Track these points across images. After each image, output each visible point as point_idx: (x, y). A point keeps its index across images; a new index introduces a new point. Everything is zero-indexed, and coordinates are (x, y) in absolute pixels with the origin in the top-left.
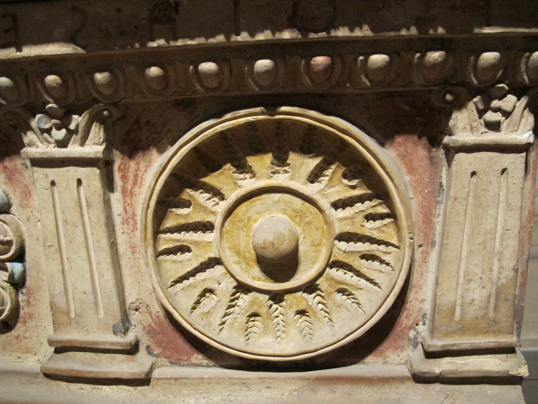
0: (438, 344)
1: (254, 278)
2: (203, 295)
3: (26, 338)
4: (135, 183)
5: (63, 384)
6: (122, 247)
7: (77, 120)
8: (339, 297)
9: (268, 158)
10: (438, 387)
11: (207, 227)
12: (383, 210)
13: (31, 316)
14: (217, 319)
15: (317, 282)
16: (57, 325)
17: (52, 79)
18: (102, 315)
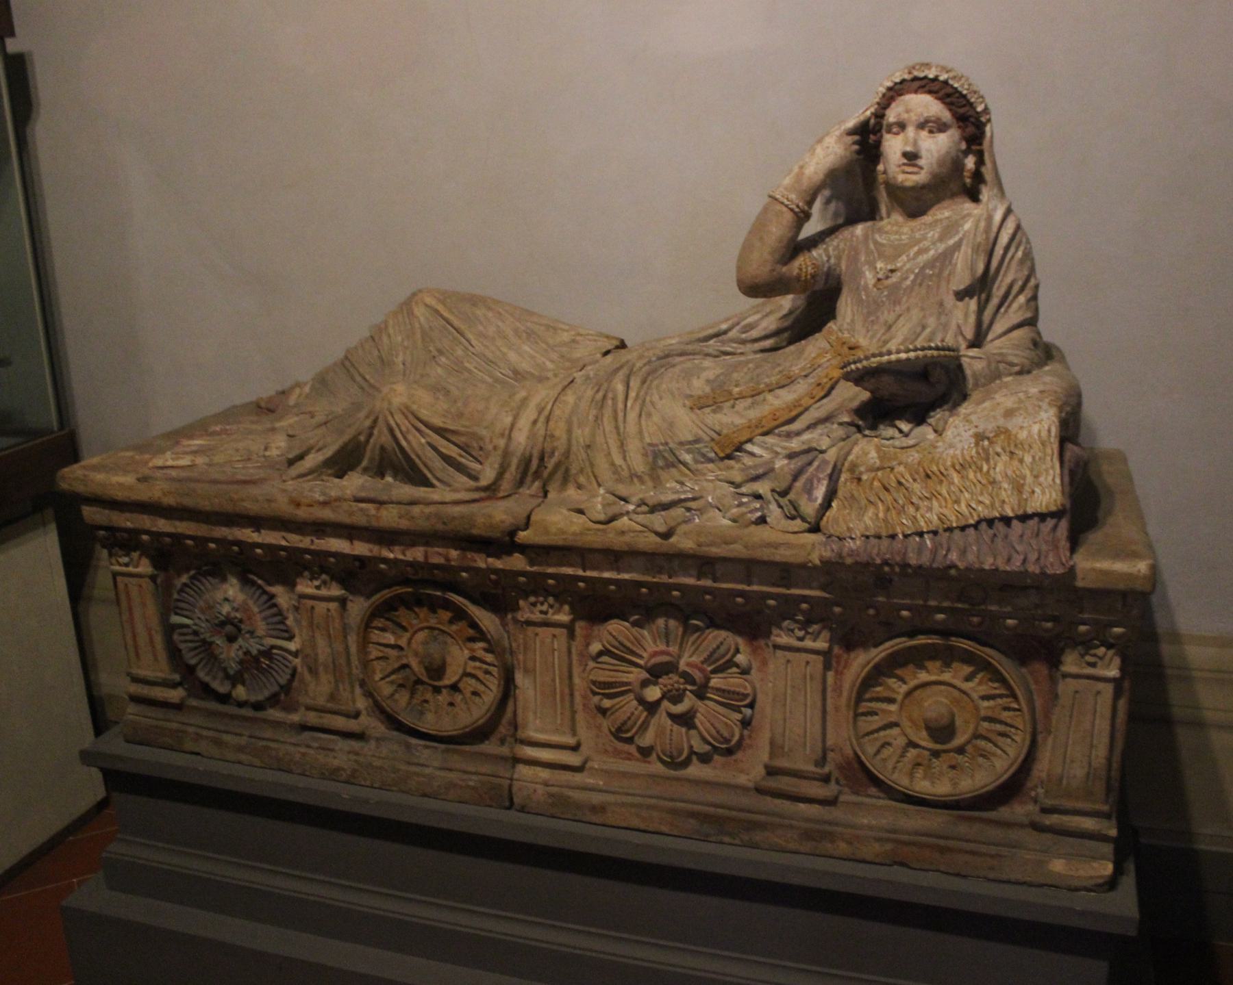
0: (1049, 802)
1: (920, 739)
2: (883, 746)
3: (742, 761)
4: (845, 668)
5: (769, 799)
6: (829, 707)
7: (815, 627)
8: (980, 760)
9: (938, 664)
10: (1049, 836)
11: (891, 701)
12: (1016, 706)
13: (750, 746)
14: (890, 765)
15: (966, 748)
16: (772, 755)
17: (804, 606)
18: (808, 752)
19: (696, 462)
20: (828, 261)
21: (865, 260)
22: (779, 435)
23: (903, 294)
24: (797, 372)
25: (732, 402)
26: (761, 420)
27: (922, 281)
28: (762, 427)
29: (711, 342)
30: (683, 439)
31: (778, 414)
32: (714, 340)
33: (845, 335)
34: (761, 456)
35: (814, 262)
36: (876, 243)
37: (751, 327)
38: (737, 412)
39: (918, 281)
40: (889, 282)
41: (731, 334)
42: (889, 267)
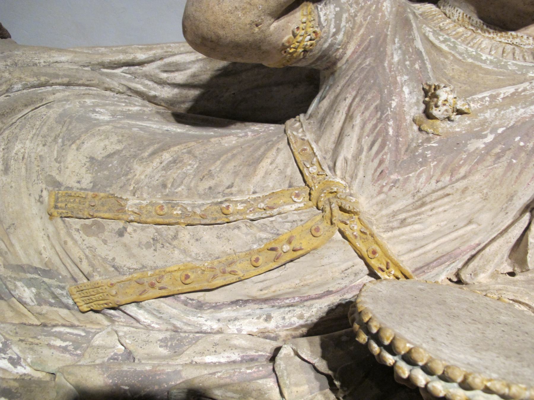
19: (41, 301)
20: (335, 34)
21: (402, 62)
22: (185, 303)
23: (465, 160)
24: (240, 207)
25: (121, 224)
26: (161, 277)
27: (504, 151)
28: (161, 289)
29: (118, 71)
30: (24, 261)
31: (192, 276)
32: (124, 68)
33: (338, 180)
34: (148, 328)
35: (318, 30)
36: (426, 38)
37: (176, 68)
38: (125, 245)
39: (497, 150)
40: (443, 126)
41: (147, 68)
42: (460, 105)
